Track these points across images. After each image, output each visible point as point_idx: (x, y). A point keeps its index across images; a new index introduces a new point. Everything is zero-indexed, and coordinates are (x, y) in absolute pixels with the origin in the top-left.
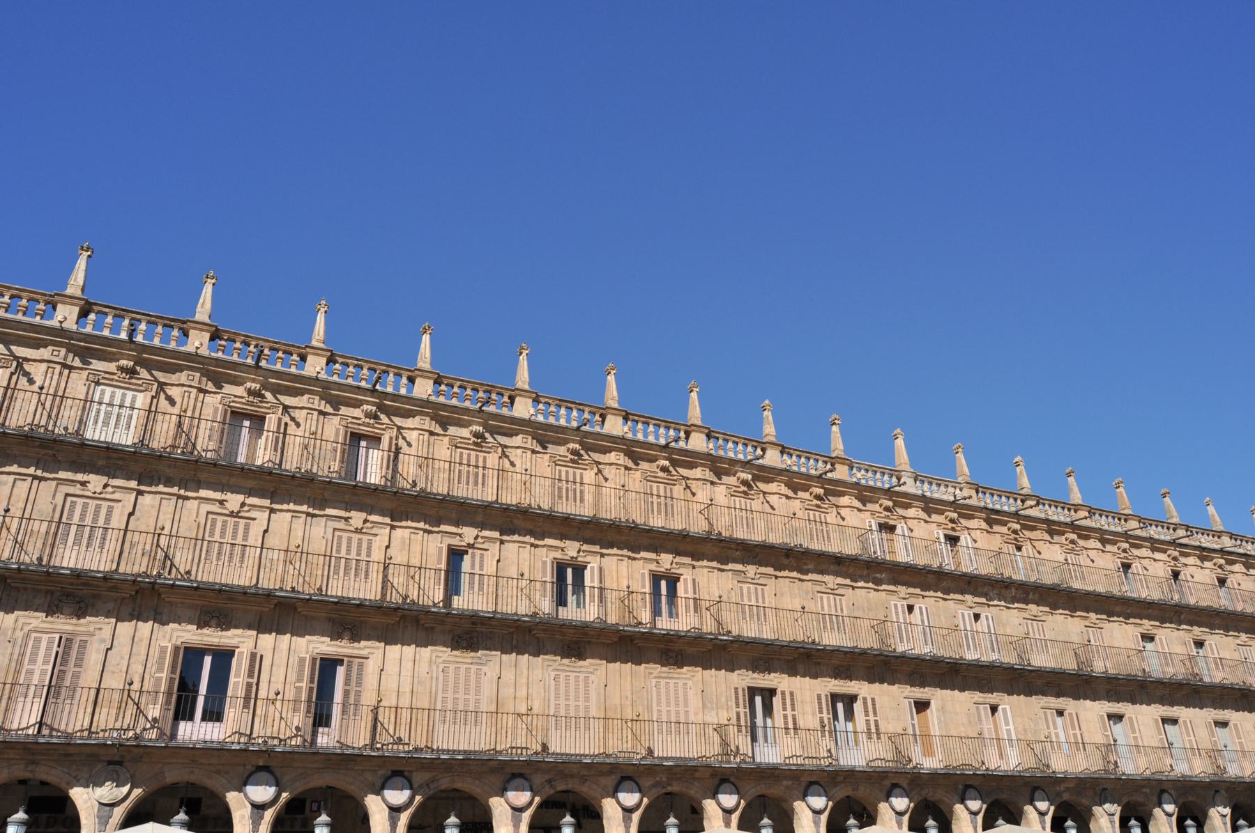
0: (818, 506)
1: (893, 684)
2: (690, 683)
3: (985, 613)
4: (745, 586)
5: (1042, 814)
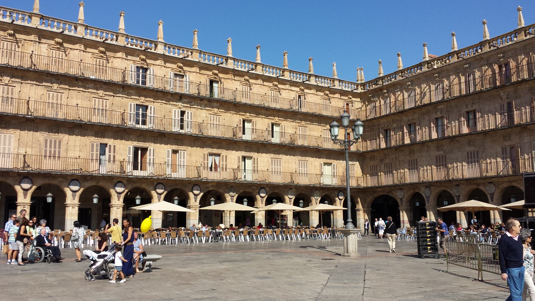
0: (101, 56)
1: (128, 140)
2: (13, 136)
3: (188, 111)
4: (51, 93)
5: (196, 195)
